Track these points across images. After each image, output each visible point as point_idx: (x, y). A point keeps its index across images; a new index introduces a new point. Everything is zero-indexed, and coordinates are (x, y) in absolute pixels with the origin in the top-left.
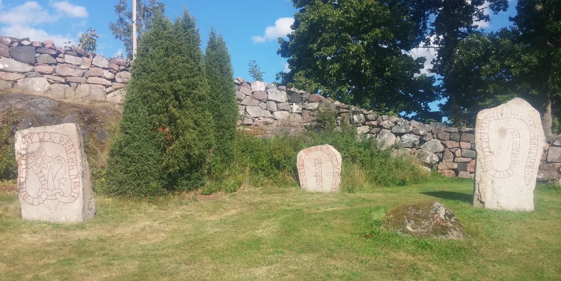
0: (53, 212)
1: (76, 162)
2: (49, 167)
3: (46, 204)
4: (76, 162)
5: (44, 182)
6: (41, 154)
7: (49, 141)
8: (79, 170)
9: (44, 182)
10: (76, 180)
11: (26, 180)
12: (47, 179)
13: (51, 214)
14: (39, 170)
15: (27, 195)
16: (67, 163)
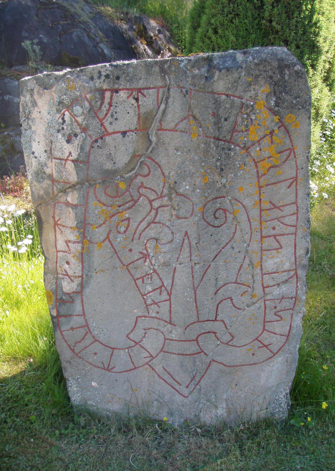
0: (186, 392)
1: (291, 220)
2: (178, 237)
3: (159, 368)
4: (291, 220)
5: (155, 296)
6: (149, 182)
7: (182, 126)
8: (301, 252)
9: (155, 296)
10: (284, 288)
11: (82, 286)
12: (167, 283)
13: (178, 398)
14: (137, 248)
15: (89, 340)
16: (255, 224)
